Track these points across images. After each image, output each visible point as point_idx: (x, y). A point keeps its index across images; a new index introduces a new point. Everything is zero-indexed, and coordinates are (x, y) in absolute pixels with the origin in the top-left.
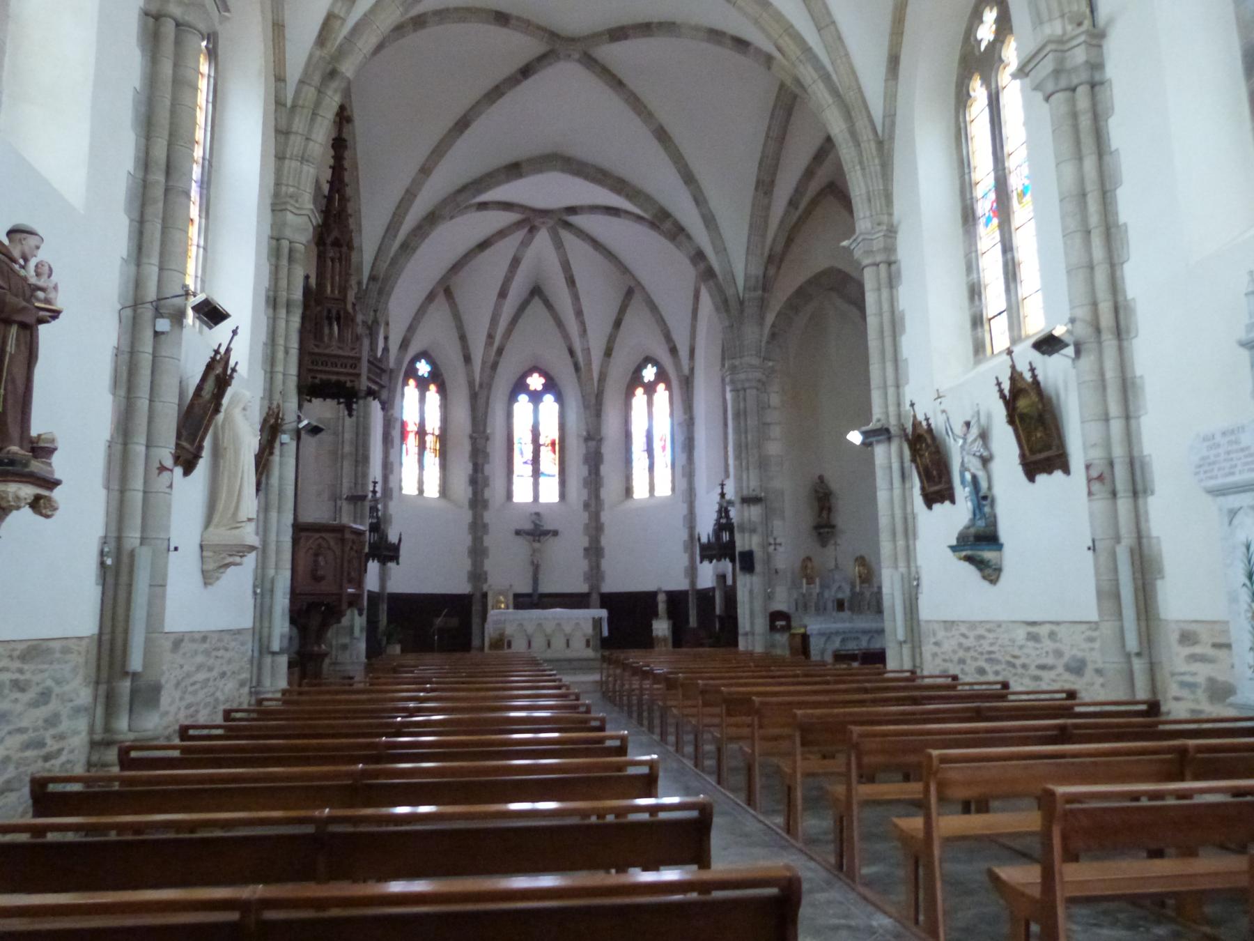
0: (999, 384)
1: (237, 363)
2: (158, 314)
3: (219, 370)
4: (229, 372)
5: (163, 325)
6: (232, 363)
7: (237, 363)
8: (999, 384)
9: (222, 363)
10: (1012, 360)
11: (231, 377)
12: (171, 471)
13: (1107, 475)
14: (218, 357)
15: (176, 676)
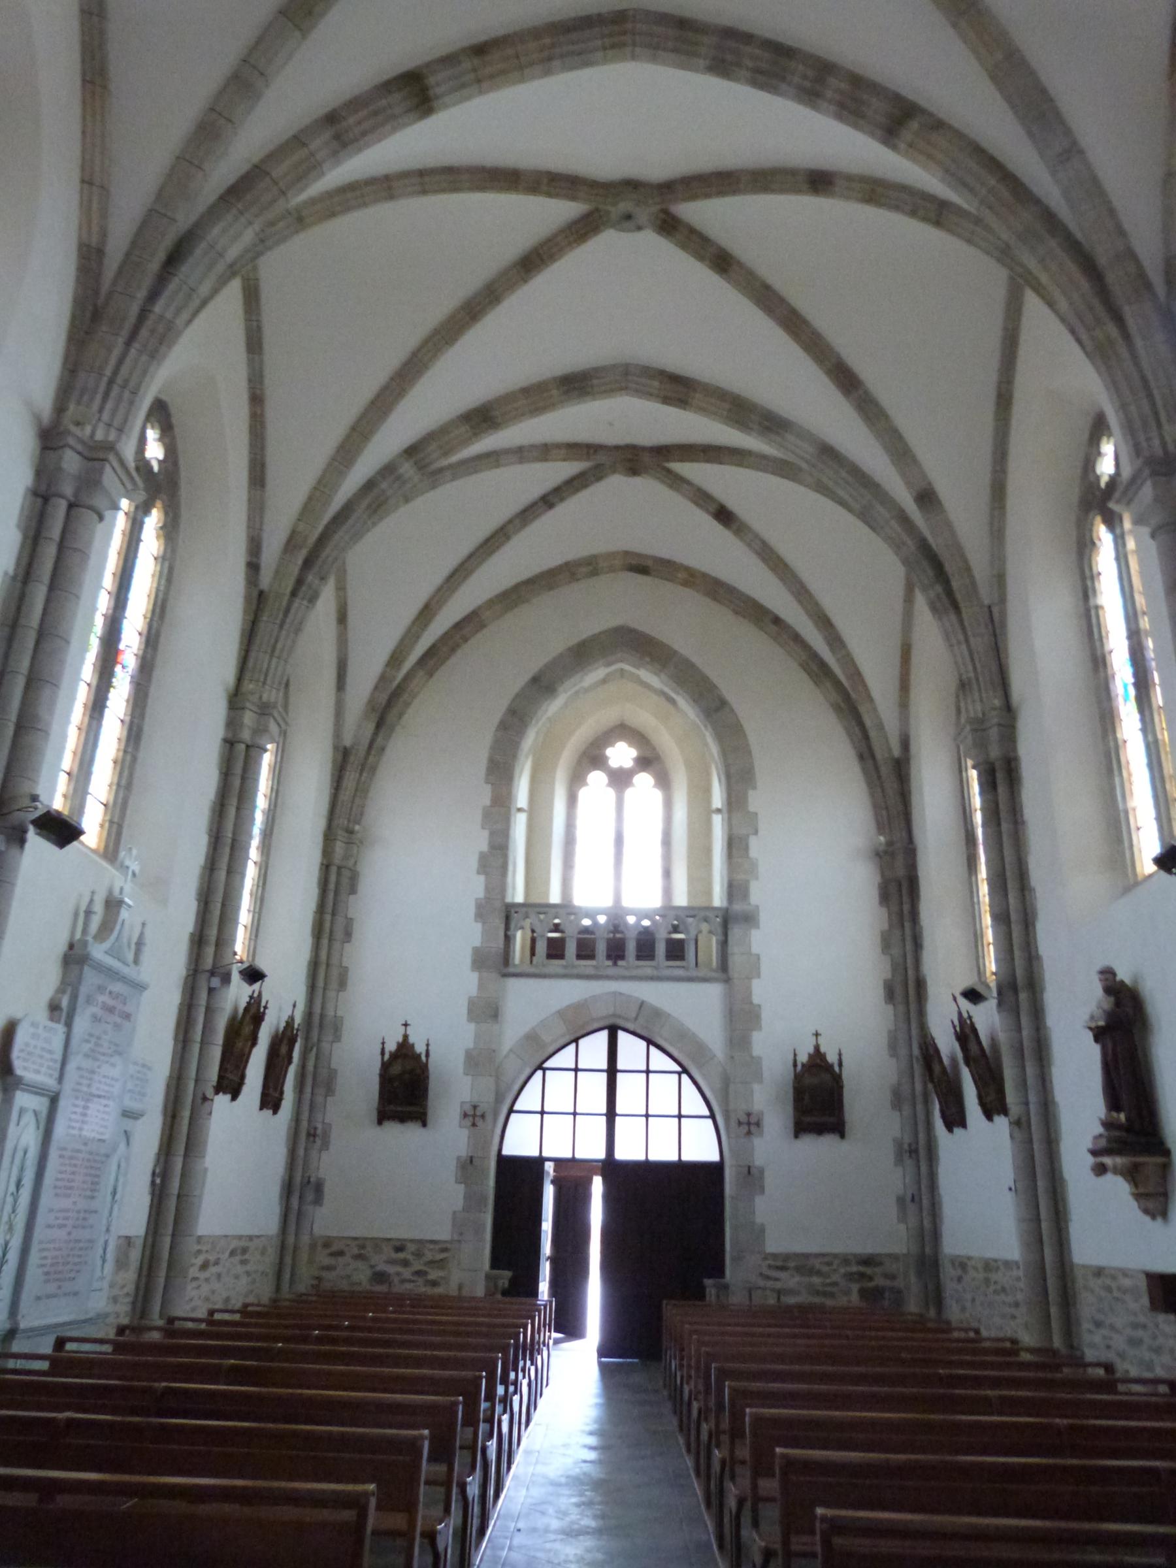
0: (953, 1023)
1: (267, 1002)
2: (212, 973)
3: (253, 1011)
4: (262, 1010)
5: (216, 982)
6: (263, 1004)
7: (267, 1002)
8: (953, 1023)
9: (255, 1005)
10: (958, 1006)
11: (264, 1013)
12: (212, 1100)
13: (1024, 1119)
14: (253, 1001)
15: (213, 1292)
